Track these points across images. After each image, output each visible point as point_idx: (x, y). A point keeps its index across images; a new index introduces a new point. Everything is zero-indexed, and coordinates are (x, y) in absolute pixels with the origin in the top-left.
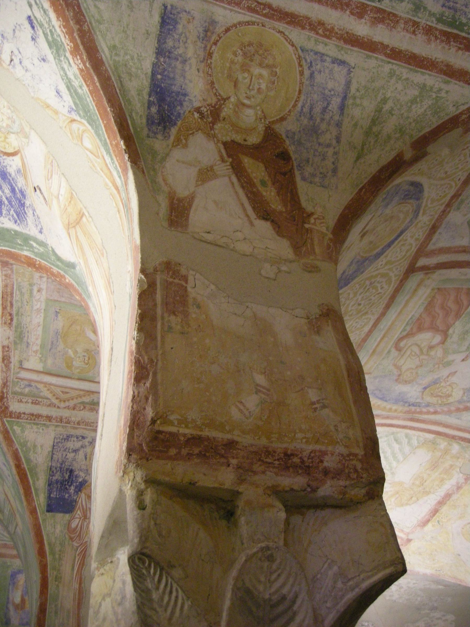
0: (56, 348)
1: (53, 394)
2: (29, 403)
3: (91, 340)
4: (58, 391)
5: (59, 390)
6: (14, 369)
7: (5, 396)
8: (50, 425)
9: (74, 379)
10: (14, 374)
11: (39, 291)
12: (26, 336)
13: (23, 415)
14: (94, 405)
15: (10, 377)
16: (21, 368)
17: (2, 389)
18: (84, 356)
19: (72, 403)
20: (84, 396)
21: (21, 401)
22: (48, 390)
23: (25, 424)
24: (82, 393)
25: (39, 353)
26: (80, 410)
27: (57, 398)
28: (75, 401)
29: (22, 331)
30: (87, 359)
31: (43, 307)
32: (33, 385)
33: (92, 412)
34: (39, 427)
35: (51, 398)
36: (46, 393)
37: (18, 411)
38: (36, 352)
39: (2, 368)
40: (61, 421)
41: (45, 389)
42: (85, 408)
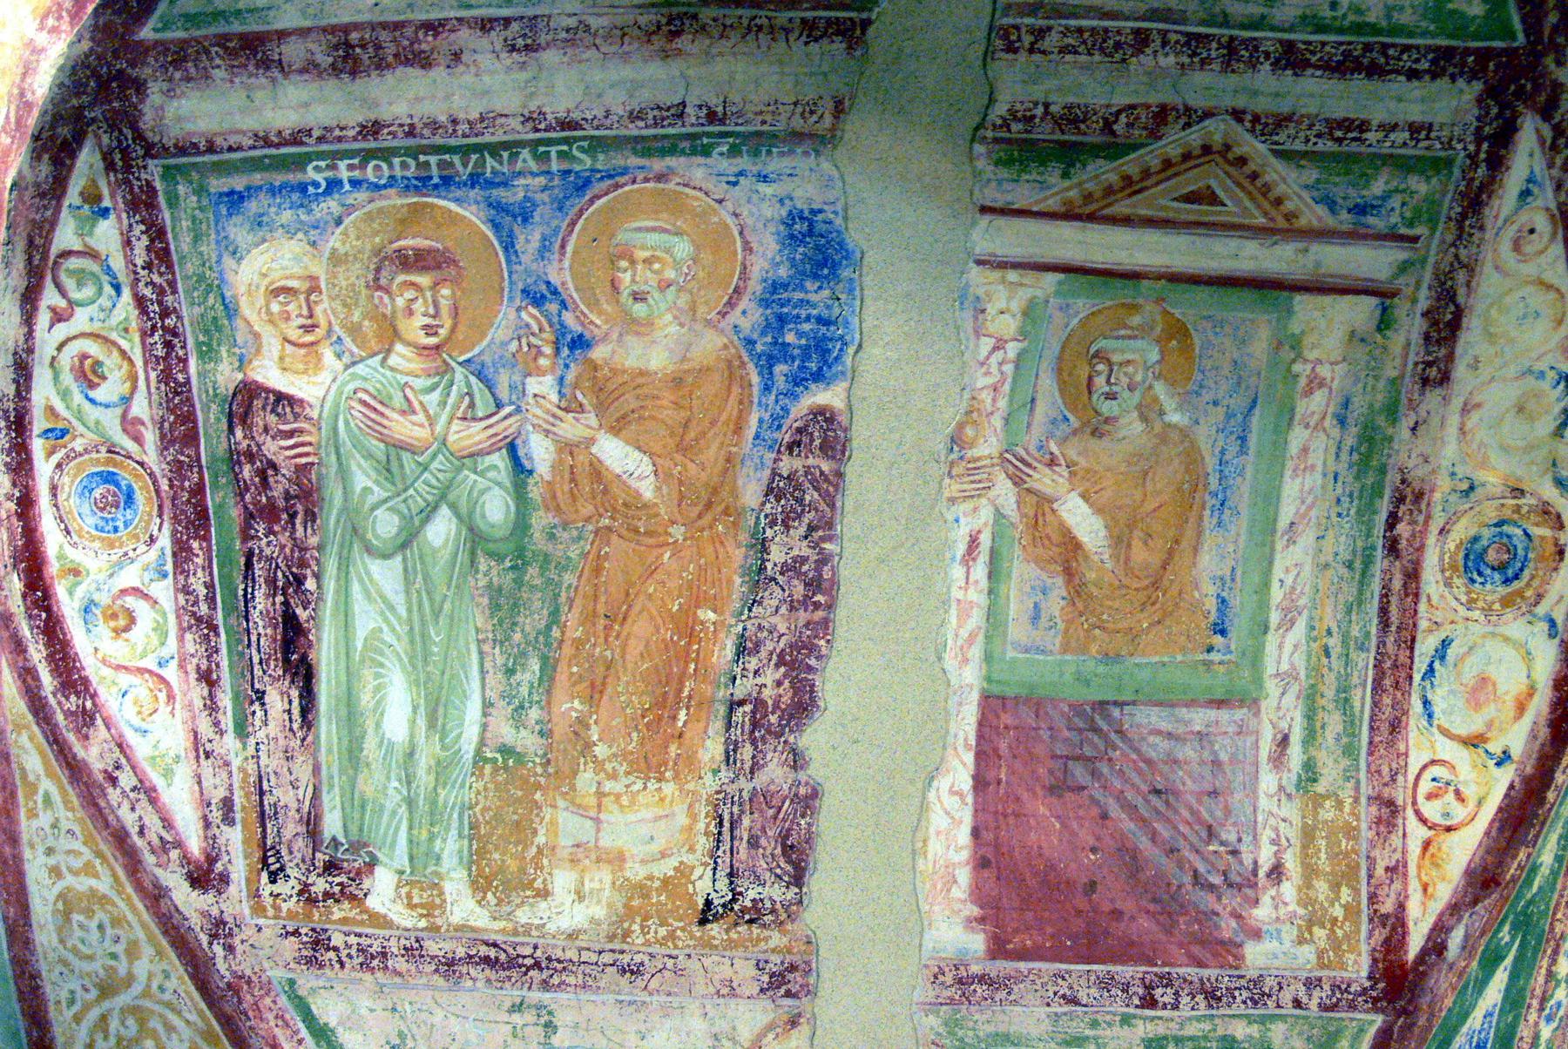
0: (1229, 416)
1: (1259, 183)
2: (1381, 127)
3: (1084, 496)
4: (1237, 203)
5: (1231, 207)
6: (1418, 285)
7: (1485, 146)
8: (1291, 29)
9: (1160, 277)
10: (1424, 262)
11: (1284, 741)
12: (1344, 456)
13: (1424, 65)
14: (1063, 144)
15: (1443, 241)
16: (1383, 294)
17: (1492, 179)
18: (1111, 396)
19: (1174, 142)
20: (1109, 191)
21: (1414, 129)
22: (1278, 202)
23: (1424, 24)
24: (1122, 208)
25: (1303, 381)
26: (1133, 107)
27: (1242, 161)
28: (1150, 156)
29: (1357, 478)
30: (1100, 381)
31: (1271, 640)
32: (1344, 215)
33: (1069, 107)
34: (1351, 18)
35: (1272, 160)
36: (1290, 181)
37: (1443, 83)
38: (1316, 383)
39: (1468, 284)
40: (1231, 50)
41: (1289, 206)
42: (1108, 126)
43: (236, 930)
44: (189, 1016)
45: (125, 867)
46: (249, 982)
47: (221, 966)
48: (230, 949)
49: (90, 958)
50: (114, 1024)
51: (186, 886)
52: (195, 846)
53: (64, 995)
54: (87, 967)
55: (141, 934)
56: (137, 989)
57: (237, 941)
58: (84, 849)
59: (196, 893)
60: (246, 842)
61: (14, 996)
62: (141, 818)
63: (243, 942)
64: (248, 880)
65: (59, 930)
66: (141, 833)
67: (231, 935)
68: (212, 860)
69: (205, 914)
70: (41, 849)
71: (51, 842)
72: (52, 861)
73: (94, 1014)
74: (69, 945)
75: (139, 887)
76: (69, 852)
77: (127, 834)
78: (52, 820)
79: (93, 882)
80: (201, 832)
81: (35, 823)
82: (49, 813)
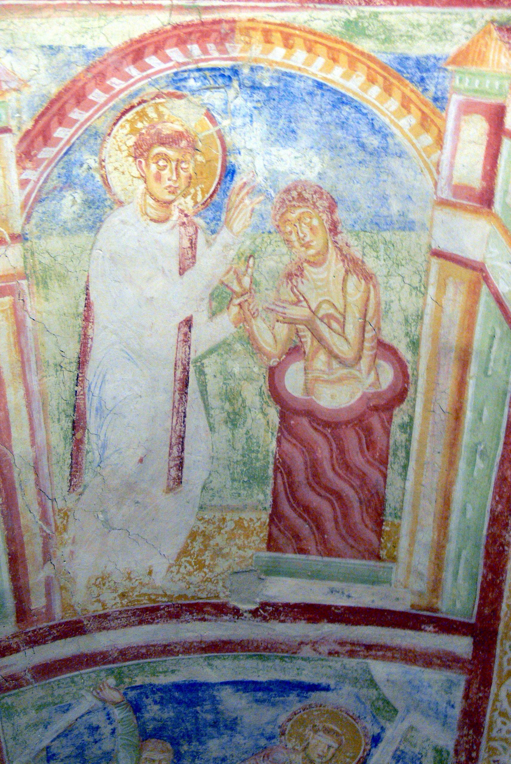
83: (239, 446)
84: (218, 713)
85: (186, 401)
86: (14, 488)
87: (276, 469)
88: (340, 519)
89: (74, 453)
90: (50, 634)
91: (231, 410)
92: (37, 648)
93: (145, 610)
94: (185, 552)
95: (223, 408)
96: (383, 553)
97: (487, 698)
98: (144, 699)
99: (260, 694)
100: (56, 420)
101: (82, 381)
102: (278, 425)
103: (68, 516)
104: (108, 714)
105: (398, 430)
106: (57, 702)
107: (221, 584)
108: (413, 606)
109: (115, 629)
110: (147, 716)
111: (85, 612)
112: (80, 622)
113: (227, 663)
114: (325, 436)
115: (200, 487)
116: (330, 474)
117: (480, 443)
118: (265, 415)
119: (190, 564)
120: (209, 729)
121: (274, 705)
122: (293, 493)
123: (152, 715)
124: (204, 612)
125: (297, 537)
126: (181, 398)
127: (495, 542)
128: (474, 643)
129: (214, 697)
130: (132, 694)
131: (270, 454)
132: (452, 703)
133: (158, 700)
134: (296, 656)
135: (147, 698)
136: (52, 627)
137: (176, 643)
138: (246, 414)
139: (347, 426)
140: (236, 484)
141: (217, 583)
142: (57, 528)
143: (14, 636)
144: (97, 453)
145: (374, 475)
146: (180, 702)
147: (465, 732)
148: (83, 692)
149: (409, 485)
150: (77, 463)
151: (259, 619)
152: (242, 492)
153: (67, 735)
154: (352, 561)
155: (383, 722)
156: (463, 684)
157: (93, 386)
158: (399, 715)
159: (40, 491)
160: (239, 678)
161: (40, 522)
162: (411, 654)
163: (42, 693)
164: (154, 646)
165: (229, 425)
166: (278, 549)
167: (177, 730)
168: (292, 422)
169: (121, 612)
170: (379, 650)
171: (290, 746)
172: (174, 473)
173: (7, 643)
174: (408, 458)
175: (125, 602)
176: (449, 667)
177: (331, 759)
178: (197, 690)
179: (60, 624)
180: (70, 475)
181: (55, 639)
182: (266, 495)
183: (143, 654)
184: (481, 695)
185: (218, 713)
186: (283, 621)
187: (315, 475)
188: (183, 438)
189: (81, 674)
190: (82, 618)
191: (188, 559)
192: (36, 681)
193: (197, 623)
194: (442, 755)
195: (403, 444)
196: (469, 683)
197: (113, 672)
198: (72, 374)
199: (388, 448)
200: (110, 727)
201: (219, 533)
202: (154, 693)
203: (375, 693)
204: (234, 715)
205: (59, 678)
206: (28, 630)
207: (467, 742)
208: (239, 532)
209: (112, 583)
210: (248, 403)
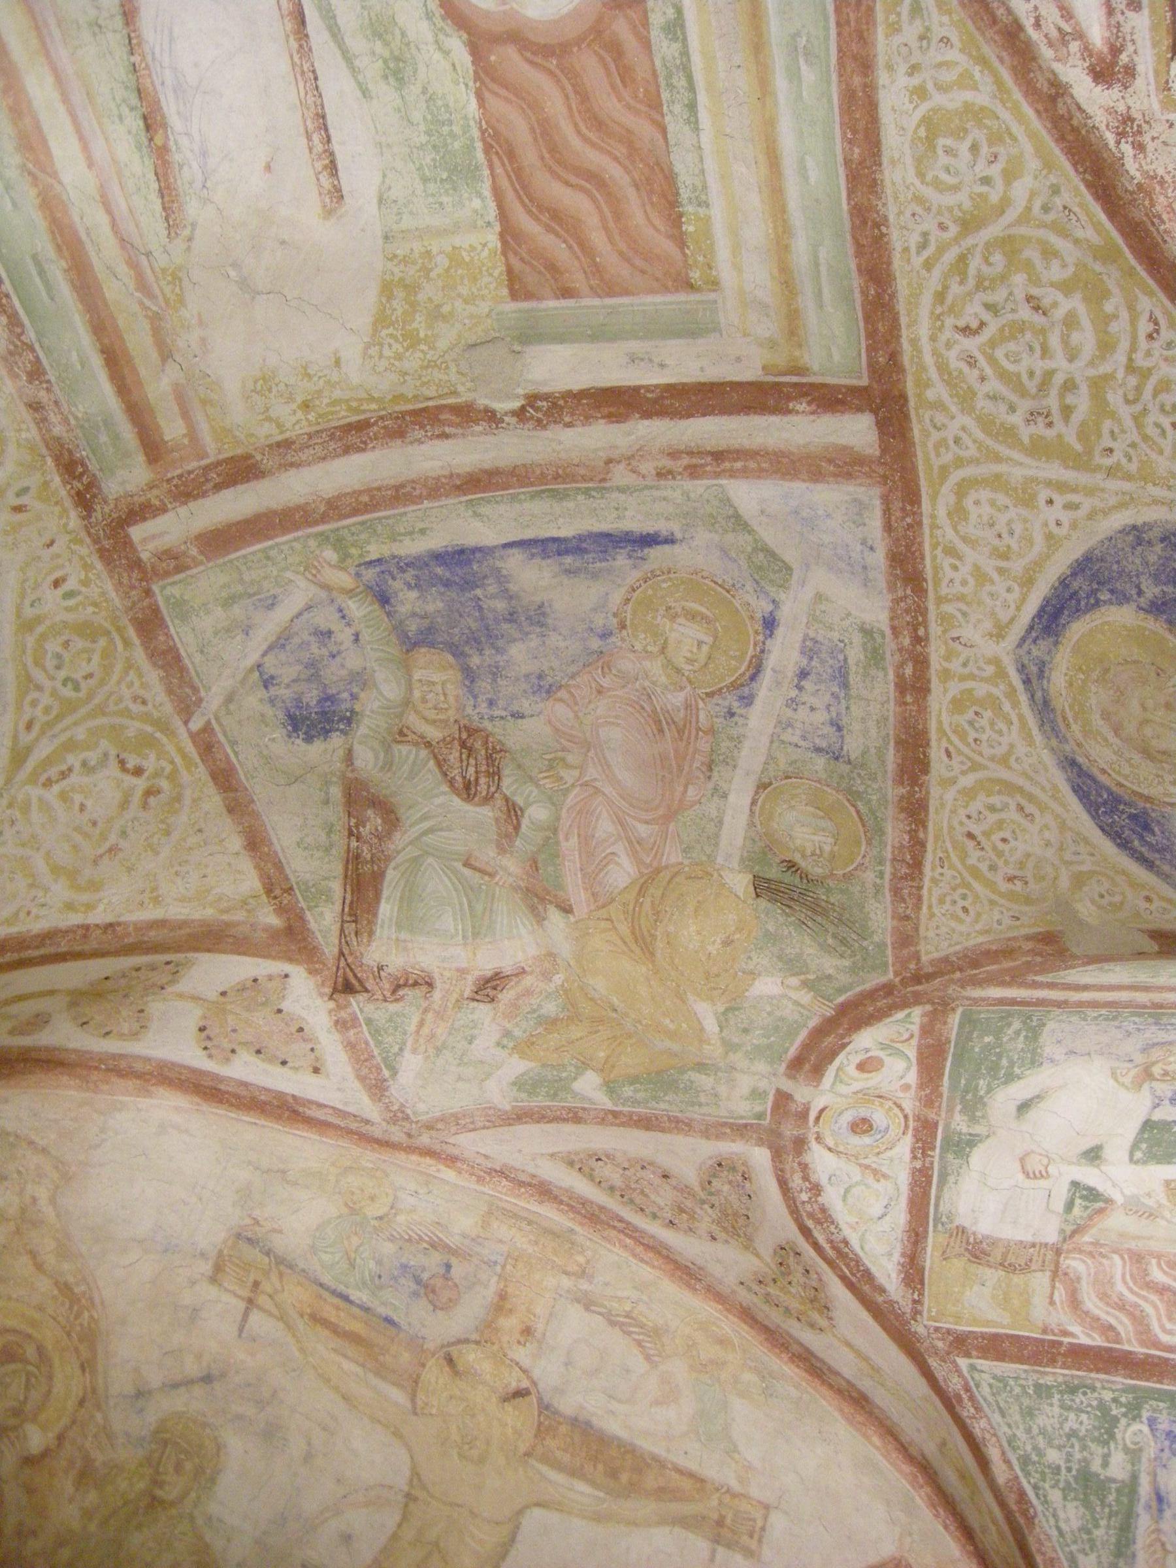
43: (1145, 127)
44: (1080, 234)
45: (1013, 69)
46: (1162, 182)
47: (1131, 166)
48: (1140, 147)
49: (955, 188)
50: (975, 264)
51: (1088, 81)
52: (1097, 35)
53: (914, 239)
54: (949, 200)
55: (1028, 147)
56: (1011, 215)
57: (1146, 138)
58: (962, 59)
59: (1099, 88)
60: (1154, 28)
61: (850, 248)
62: (1036, 8)
63: (1153, 139)
64: (1157, 73)
65: (918, 161)
66: (1037, 25)
67: (1140, 132)
68: (1116, 51)
69: (1111, 111)
70: (902, 69)
71: (917, 57)
72: (916, 81)
73: (950, 256)
74: (929, 178)
75: (1030, 90)
76: (940, 65)
77: (1020, 28)
78: (921, 29)
79: (968, 96)
80: (1104, 19)
81: (897, 40)
82: (918, 22)
83: (417, 116)
84: (511, 597)
85: (310, 50)
86: (80, 241)
87: (488, 149)
88: (611, 224)
89: (160, 171)
90: (207, 480)
91: (387, 54)
92: (192, 505)
93: (349, 428)
94: (381, 320)
95: (373, 53)
96: (695, 275)
97: (920, 524)
98: (390, 582)
99: (568, 560)
100: (117, 120)
101: (139, 44)
102: (471, 69)
103: (180, 280)
104: (341, 611)
105: (662, 36)
106: (251, 591)
107: (454, 369)
108: (764, 368)
109: (309, 465)
110: (403, 609)
111: (252, 440)
112: (248, 457)
113: (502, 508)
114: (551, 73)
115: (375, 201)
116: (576, 142)
117: (797, 34)
118: (447, 53)
119: (397, 340)
120: (505, 626)
121: (595, 576)
122: (524, 187)
123: (409, 607)
124: (443, 423)
125: (552, 268)
126: (301, 46)
127: (864, 222)
128: (877, 423)
129: (498, 570)
130: (370, 574)
131: (472, 123)
132: (870, 543)
133: (413, 583)
134: (607, 485)
135: (394, 579)
136: (207, 469)
137: (413, 481)
138: (413, 58)
139: (580, 48)
140: (432, 187)
141: (447, 367)
142: (167, 301)
143: (151, 486)
144: (195, 165)
145: (644, 129)
146: (447, 584)
147: (900, 593)
148: (289, 575)
149: (706, 138)
150: (168, 188)
151: (530, 425)
152: (445, 199)
153: (283, 646)
154: (650, 299)
155: (772, 590)
156: (877, 502)
157: (157, 50)
158: (795, 577)
159: (123, 242)
160: (529, 534)
161: (137, 294)
162: (785, 460)
163: (223, 579)
164: (379, 489)
165: (391, 80)
166: (529, 296)
167: (456, 630)
168: (493, 58)
169: (310, 436)
170: (735, 460)
171: (638, 647)
172: (326, 181)
173: (143, 499)
174: (691, 88)
175: (312, 416)
176: (849, 476)
177: (706, 665)
178: (469, 562)
179: (219, 463)
180: (164, 208)
181: (218, 487)
182: (483, 199)
183: (366, 505)
184: (909, 520)
185: (511, 597)
186: (569, 425)
187: (553, 150)
188: (324, 117)
189: (277, 544)
190: (250, 450)
191: (391, 330)
192: (209, 559)
193: (436, 442)
194: (874, 639)
195: (678, 62)
196: (886, 500)
197: (327, 538)
198: (118, 36)
199: (655, 74)
200: (349, 632)
201: (429, 279)
202: (402, 570)
203: (749, 538)
204: (538, 599)
205: (243, 552)
206: (169, 475)
207: (907, 611)
208: (460, 272)
209: (282, 387)
210: (412, 36)
